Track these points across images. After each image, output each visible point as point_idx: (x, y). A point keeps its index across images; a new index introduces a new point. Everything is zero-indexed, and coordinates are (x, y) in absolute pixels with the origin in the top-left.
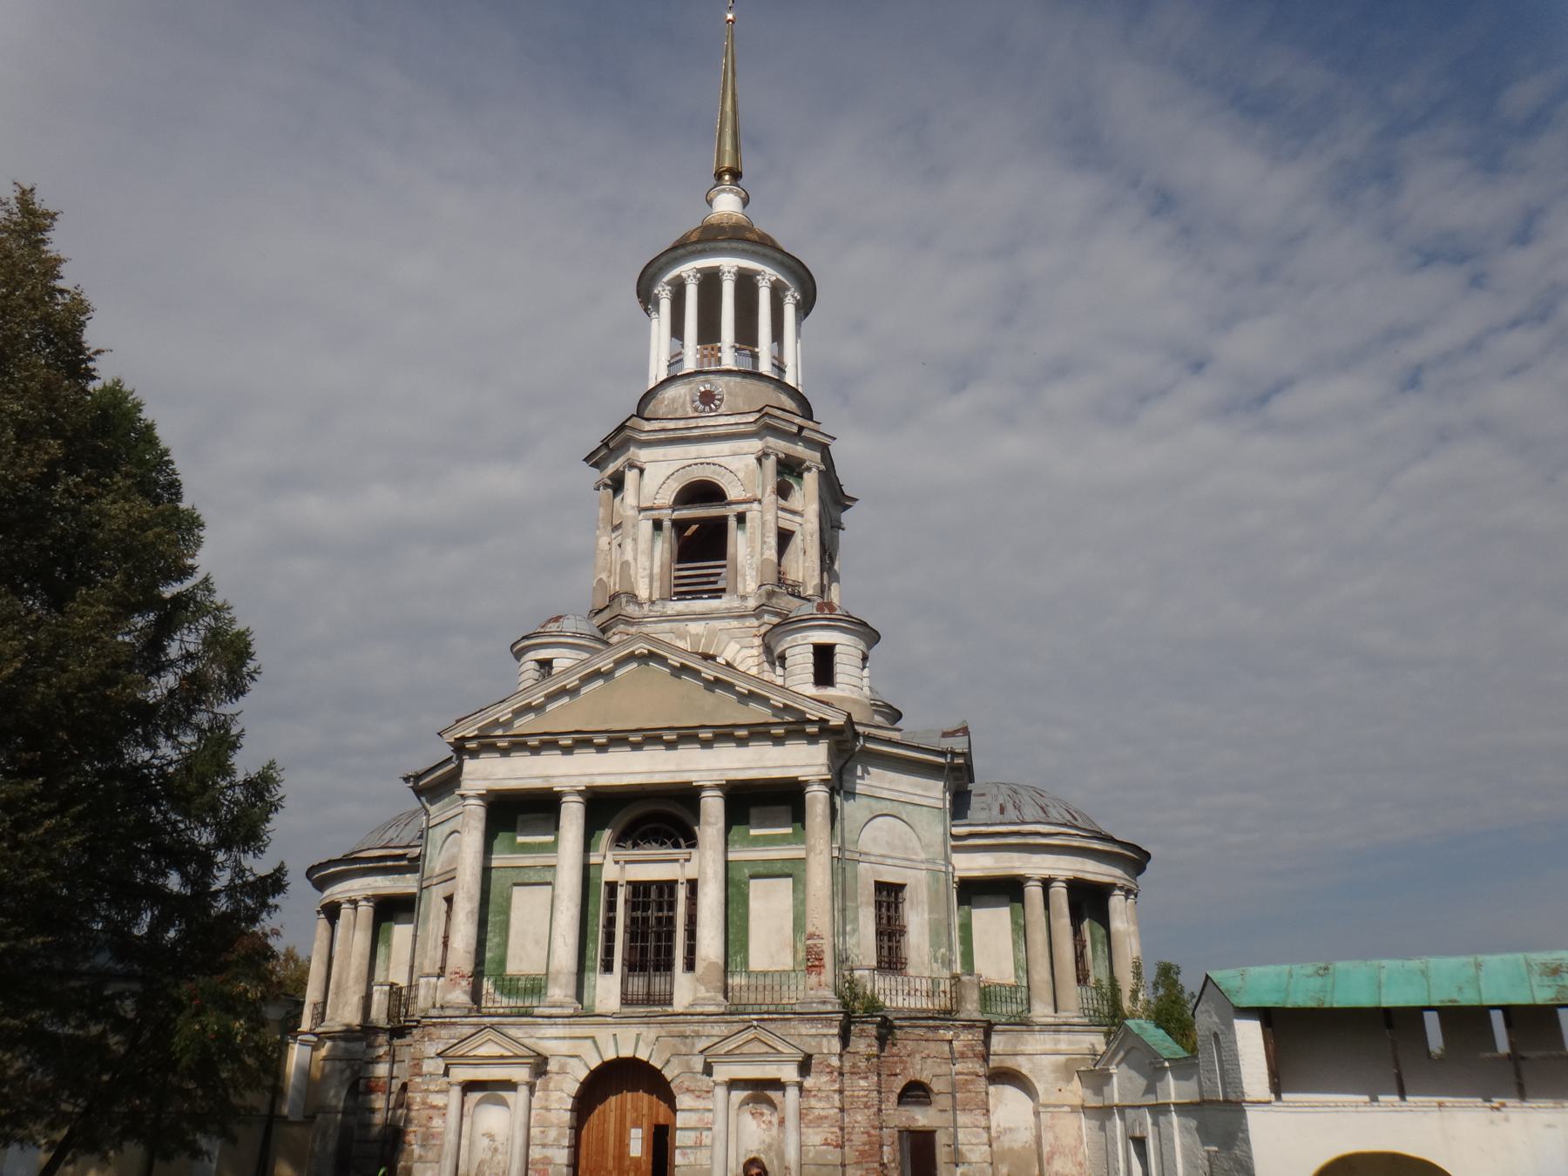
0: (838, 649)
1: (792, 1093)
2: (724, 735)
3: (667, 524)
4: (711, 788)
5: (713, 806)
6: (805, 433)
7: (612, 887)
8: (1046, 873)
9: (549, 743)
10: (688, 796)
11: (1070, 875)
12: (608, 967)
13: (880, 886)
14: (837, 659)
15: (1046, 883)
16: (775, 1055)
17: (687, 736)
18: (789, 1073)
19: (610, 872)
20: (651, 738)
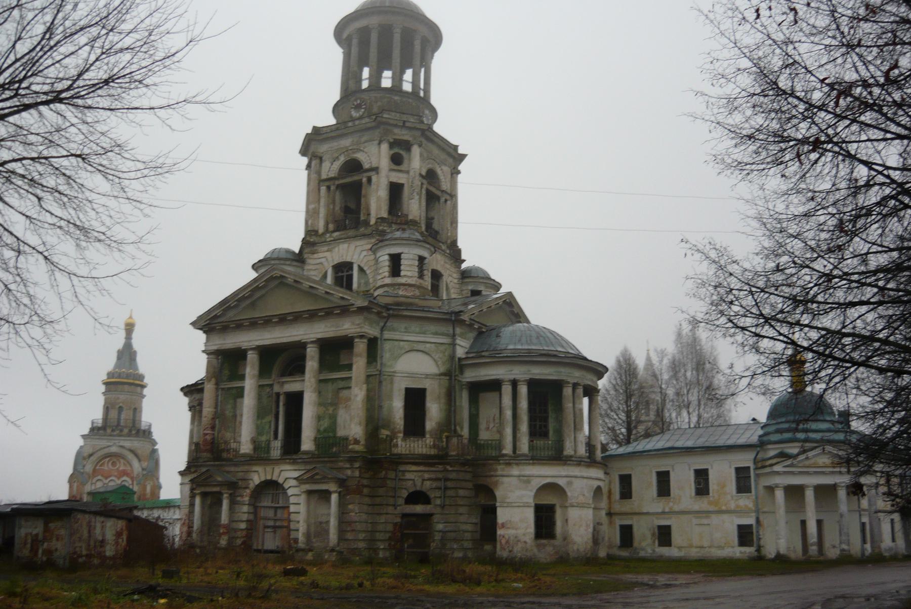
0: (403, 256)
1: (334, 497)
2: (312, 316)
3: (332, 188)
4: (312, 342)
5: (312, 352)
6: (407, 124)
7: (278, 395)
8: (512, 377)
9: (239, 326)
10: (301, 346)
11: (528, 377)
12: (276, 437)
13: (409, 391)
14: (402, 262)
15: (514, 384)
16: (325, 479)
17: (297, 318)
18: (332, 487)
19: (276, 389)
20: (283, 320)
